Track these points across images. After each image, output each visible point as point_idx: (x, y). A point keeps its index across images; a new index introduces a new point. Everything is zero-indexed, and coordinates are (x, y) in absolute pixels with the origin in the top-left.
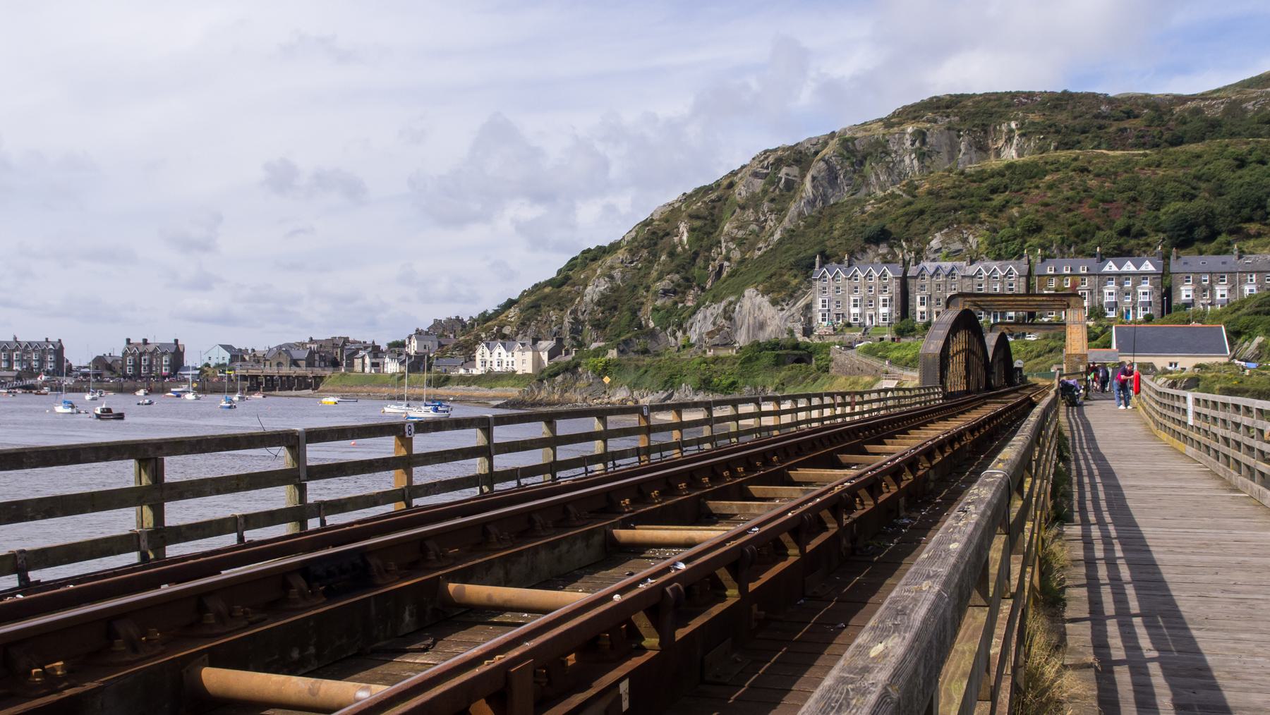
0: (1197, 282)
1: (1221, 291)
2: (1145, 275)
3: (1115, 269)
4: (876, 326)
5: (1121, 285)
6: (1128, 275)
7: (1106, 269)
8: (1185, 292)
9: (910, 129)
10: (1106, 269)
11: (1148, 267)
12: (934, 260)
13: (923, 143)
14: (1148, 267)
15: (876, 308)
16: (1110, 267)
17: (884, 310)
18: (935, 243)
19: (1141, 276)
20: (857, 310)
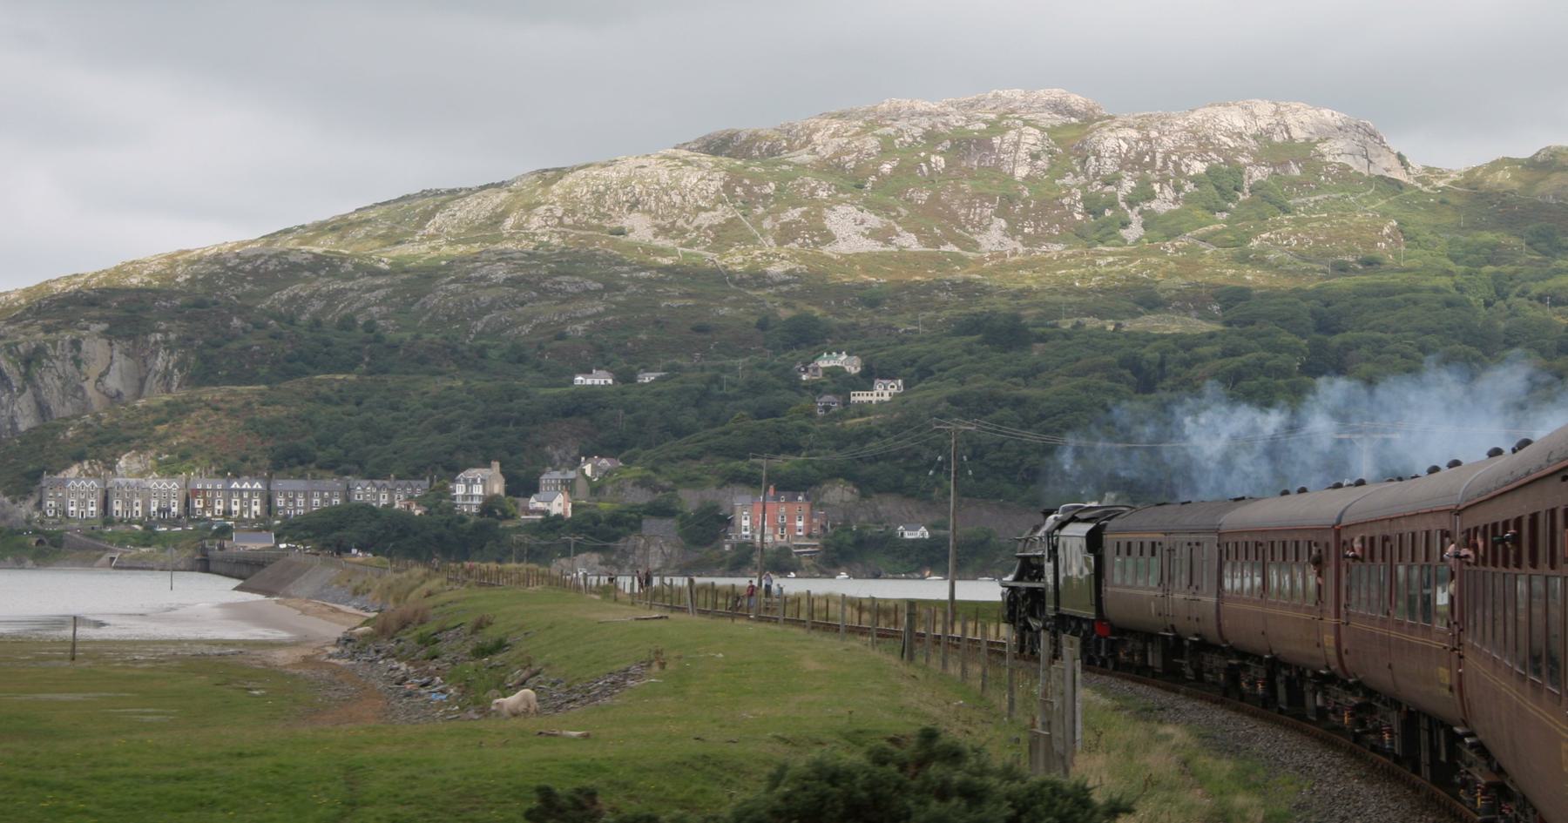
0: (286, 496)
1: (301, 500)
2: (257, 490)
3: (238, 487)
4: (87, 518)
5: (241, 496)
6: (246, 490)
7: (233, 486)
8: (280, 501)
9: (67, 338)
10: (233, 486)
11: (258, 485)
12: (123, 476)
13: (79, 349)
14: (258, 485)
15: (86, 508)
16: (235, 485)
17: (94, 509)
18: (122, 463)
19: (251, 492)
20: (74, 508)
